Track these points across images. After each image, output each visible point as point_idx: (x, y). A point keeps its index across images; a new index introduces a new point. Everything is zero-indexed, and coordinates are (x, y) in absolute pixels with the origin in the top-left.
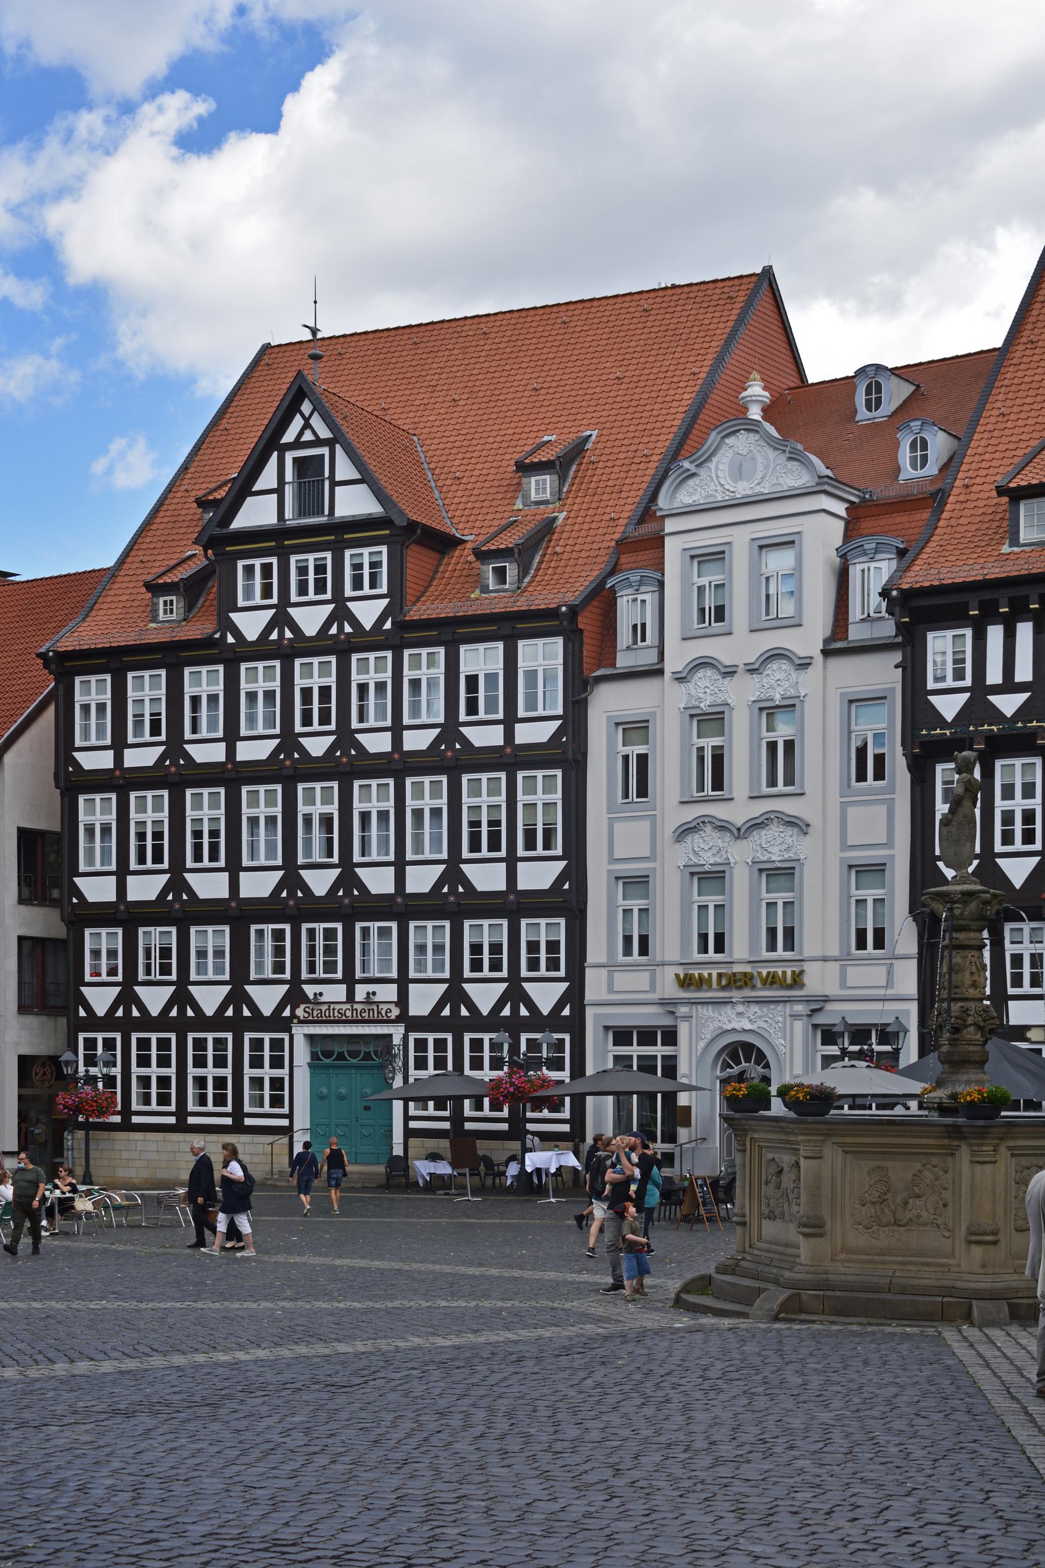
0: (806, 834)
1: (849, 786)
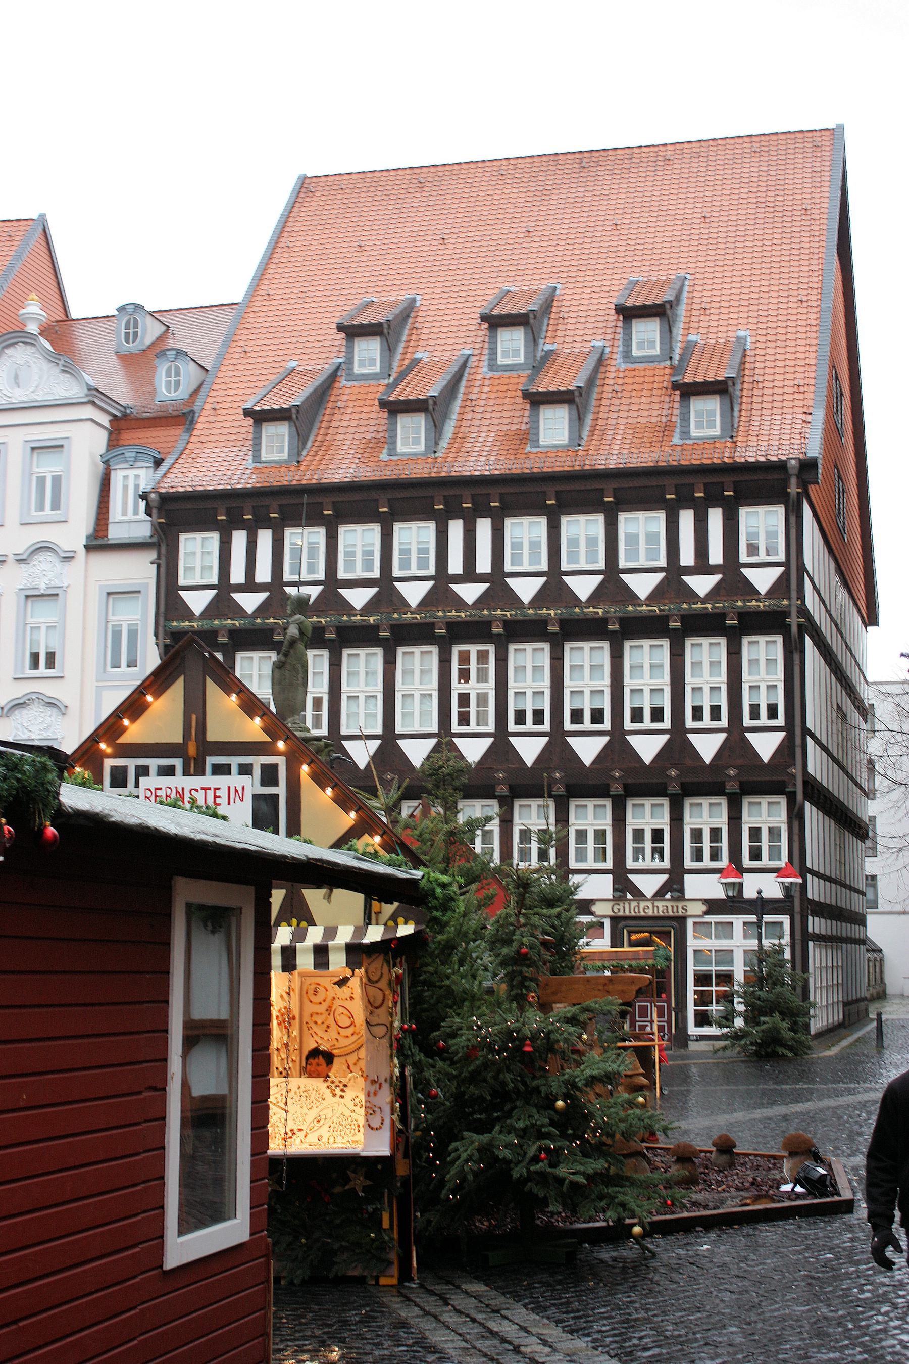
0: (64, 714)
1: (105, 671)
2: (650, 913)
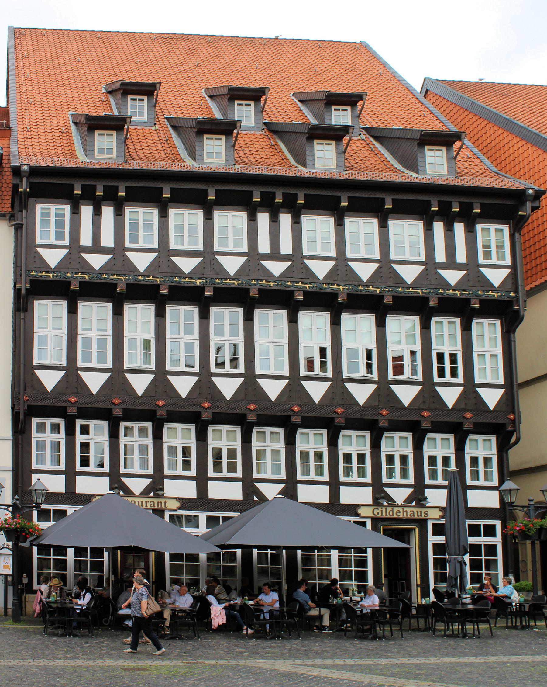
2: (401, 515)
